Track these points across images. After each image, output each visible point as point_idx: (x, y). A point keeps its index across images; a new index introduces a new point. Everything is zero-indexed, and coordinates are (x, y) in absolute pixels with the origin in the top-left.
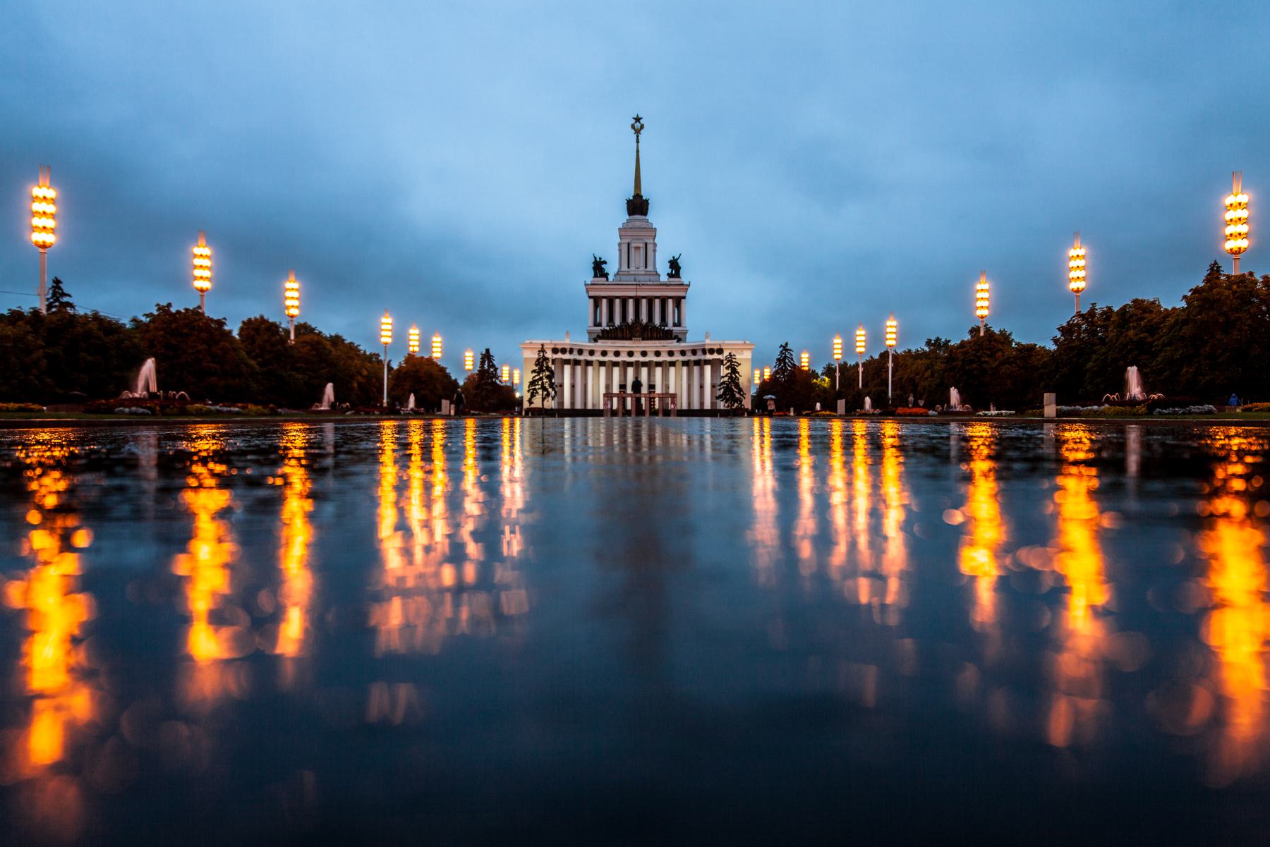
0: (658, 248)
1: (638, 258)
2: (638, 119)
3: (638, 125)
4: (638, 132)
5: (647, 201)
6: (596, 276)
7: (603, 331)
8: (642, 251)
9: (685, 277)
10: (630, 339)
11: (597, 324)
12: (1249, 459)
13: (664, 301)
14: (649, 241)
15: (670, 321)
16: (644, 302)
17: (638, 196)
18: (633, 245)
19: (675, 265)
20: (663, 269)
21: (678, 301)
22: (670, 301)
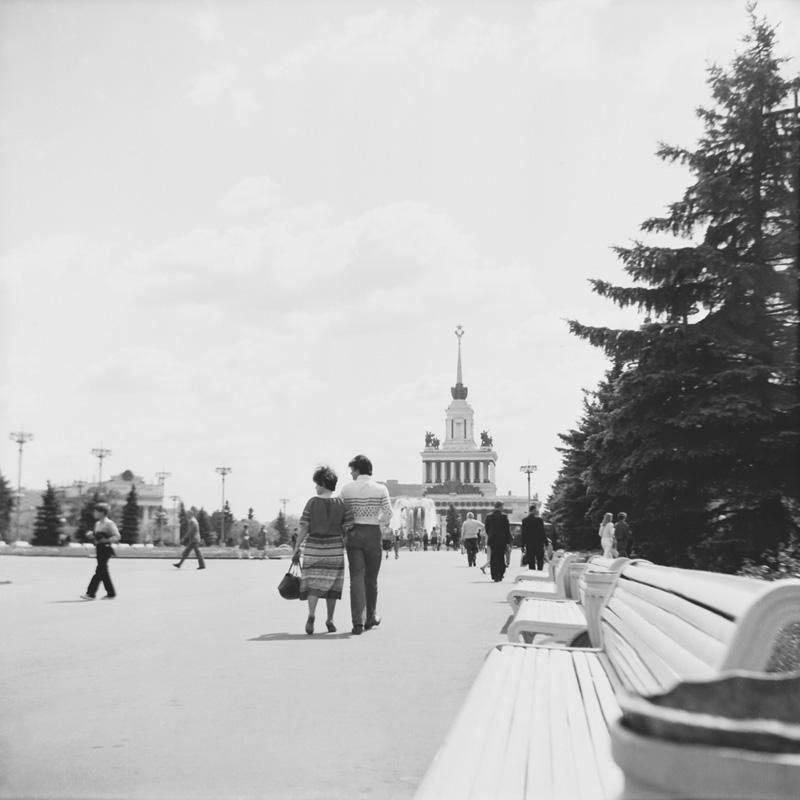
0: (475, 423)
1: (459, 431)
2: (460, 328)
3: (460, 333)
4: (460, 336)
5: (466, 389)
6: (427, 445)
7: (429, 489)
8: (463, 425)
9: (494, 448)
10: (448, 493)
11: (429, 481)
12: (772, 559)
13: (477, 463)
14: (468, 418)
15: (482, 478)
16: (462, 464)
17: (459, 385)
18: (456, 421)
19: (484, 436)
20: (479, 441)
21: (487, 463)
22: (482, 464)
